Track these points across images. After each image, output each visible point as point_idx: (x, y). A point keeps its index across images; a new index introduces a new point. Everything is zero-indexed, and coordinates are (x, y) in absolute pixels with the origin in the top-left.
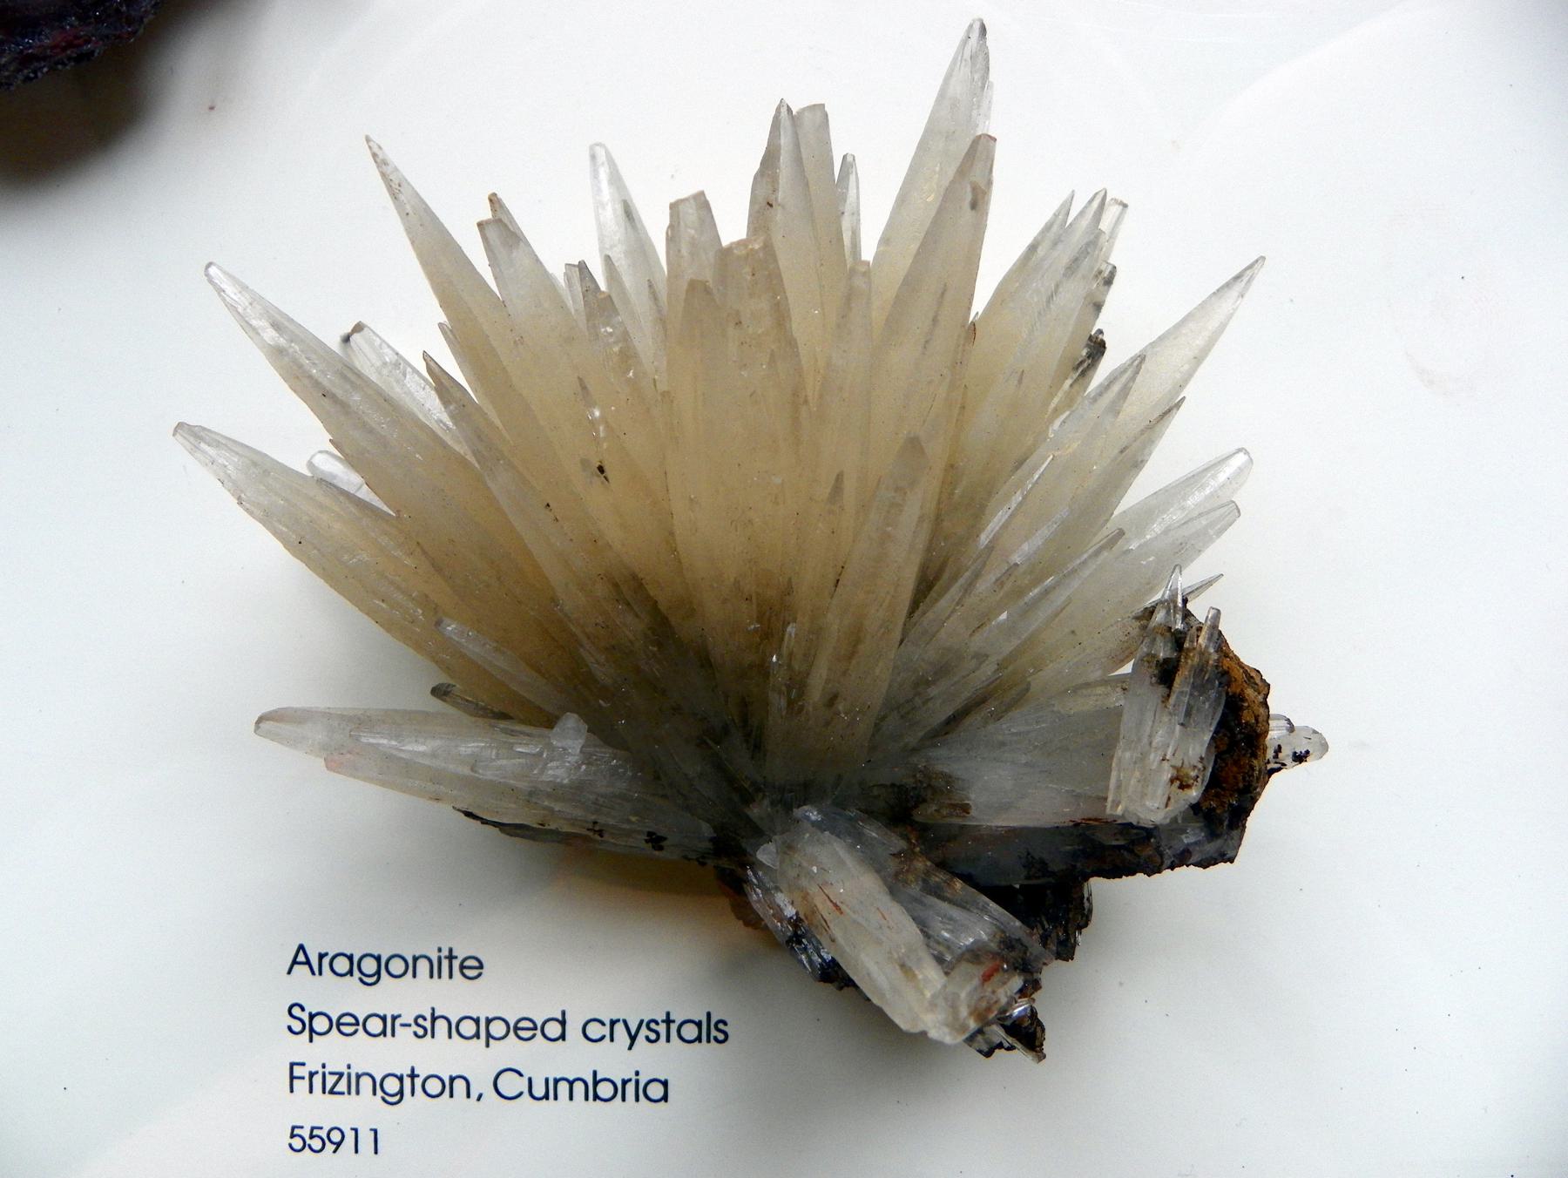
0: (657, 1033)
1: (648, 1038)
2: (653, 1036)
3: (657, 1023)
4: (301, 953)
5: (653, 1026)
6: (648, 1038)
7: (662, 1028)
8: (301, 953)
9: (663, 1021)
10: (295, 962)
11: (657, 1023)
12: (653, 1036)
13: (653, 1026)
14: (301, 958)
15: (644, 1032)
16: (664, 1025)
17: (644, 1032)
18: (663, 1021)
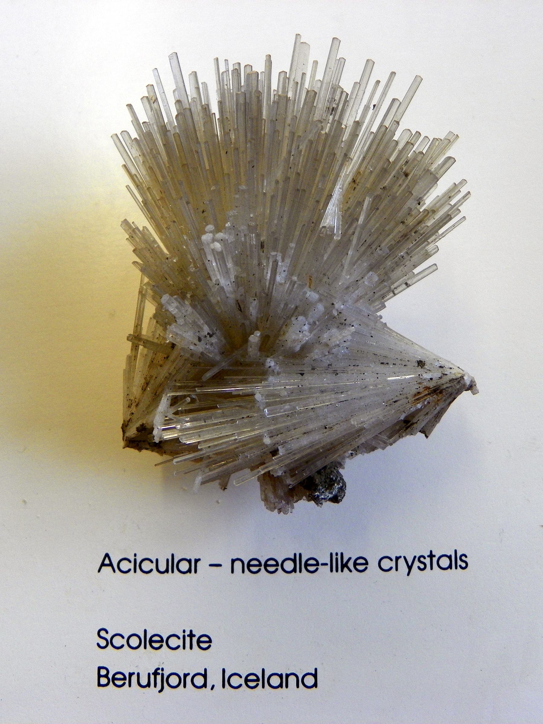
0: (425, 564)
1: (419, 568)
2: (422, 566)
3: (425, 558)
4: (107, 559)
5: (422, 559)
6: (419, 568)
7: (427, 561)
8: (107, 559)
9: (428, 556)
10: (103, 564)
11: (425, 558)
12: (422, 566)
13: (422, 559)
14: (107, 562)
15: (417, 564)
16: (429, 558)
17: (417, 564)
18: (428, 556)
